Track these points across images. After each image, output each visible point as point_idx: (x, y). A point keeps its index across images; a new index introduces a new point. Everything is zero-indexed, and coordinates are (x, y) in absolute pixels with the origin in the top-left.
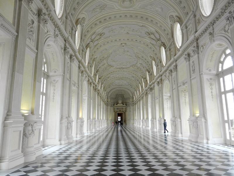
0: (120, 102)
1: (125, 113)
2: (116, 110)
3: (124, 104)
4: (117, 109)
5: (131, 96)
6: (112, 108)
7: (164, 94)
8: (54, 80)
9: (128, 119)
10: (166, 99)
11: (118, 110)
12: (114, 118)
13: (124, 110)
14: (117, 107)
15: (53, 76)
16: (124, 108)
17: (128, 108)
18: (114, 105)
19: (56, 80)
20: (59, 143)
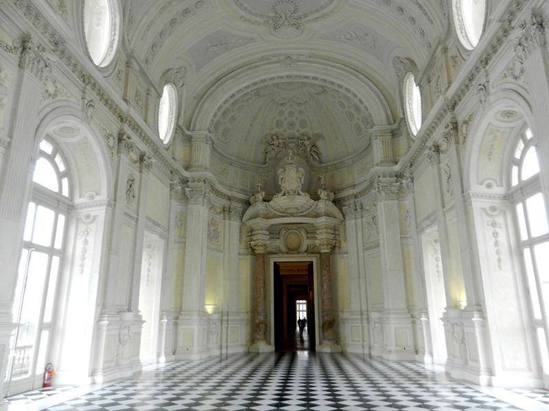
0: (292, 177)
1: (328, 261)
2: (261, 239)
3: (323, 194)
4: (274, 232)
5: (379, 115)
6: (235, 224)
7: (475, 188)
8: (88, 217)
9: (355, 306)
10: (484, 209)
11: (279, 243)
12: (244, 303)
13: (322, 238)
14: (267, 217)
15: (86, 206)
16: (323, 219)
17: (350, 223)
18: (248, 204)
19: (92, 214)
20: (89, 380)
